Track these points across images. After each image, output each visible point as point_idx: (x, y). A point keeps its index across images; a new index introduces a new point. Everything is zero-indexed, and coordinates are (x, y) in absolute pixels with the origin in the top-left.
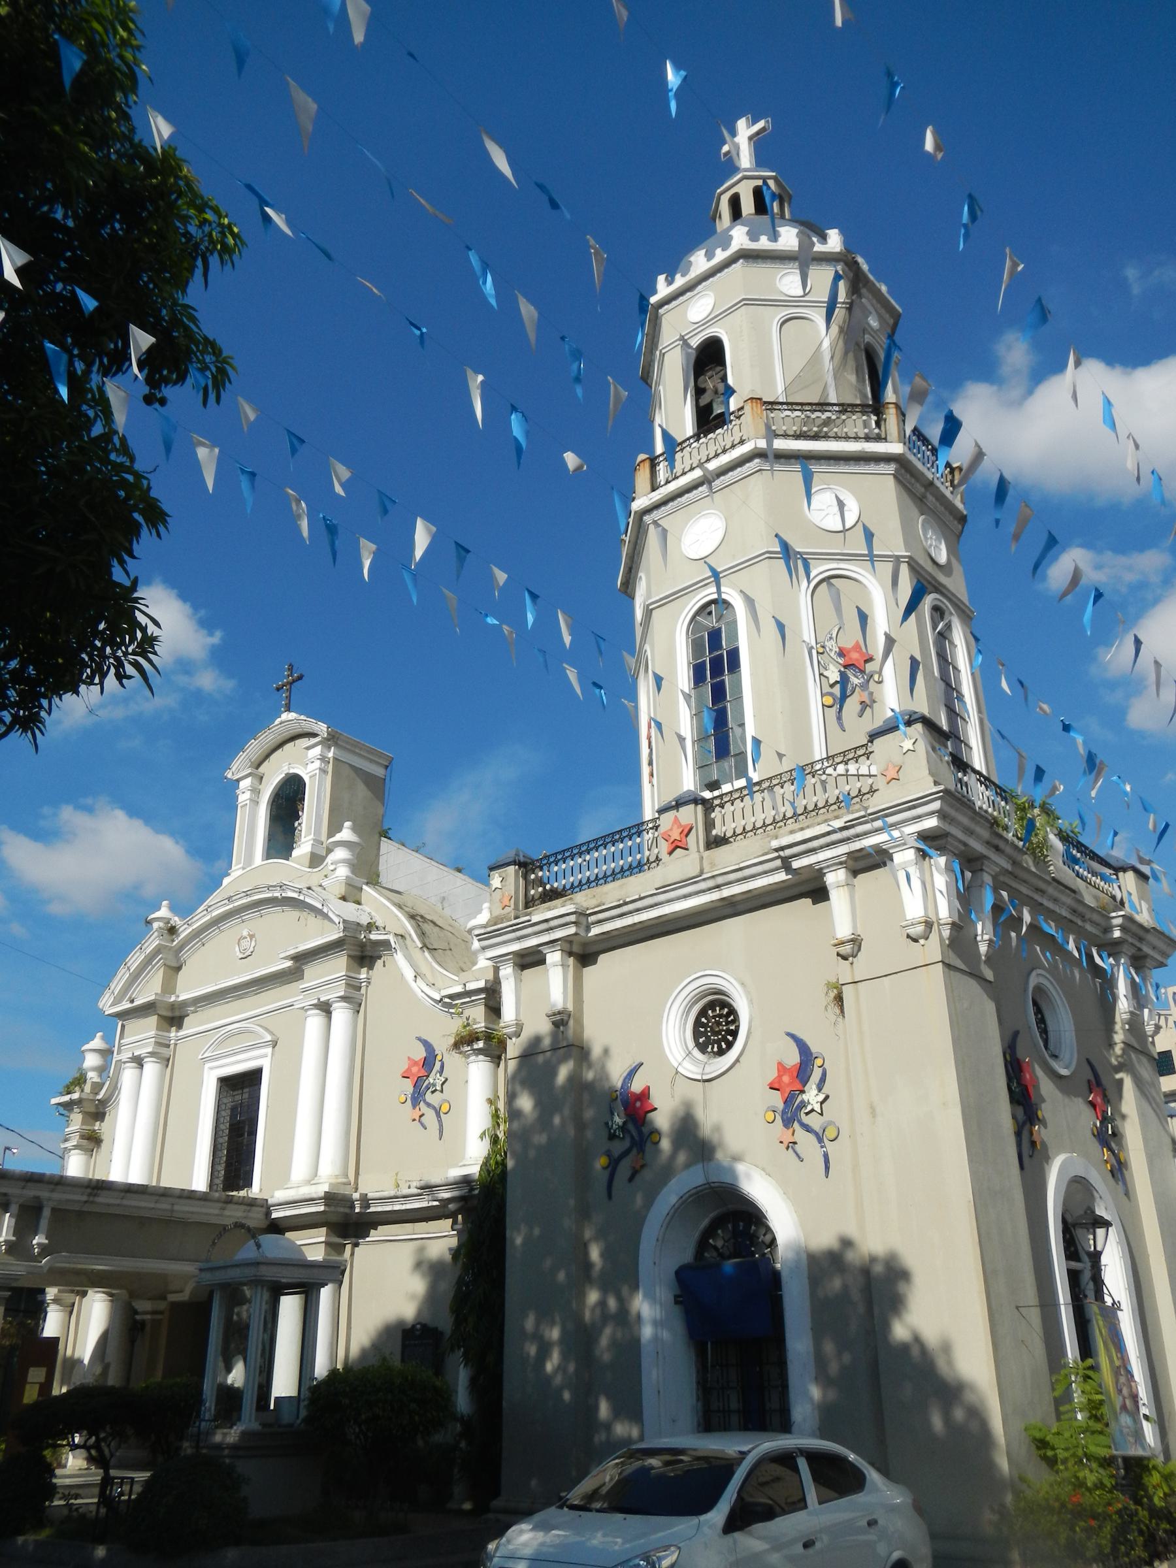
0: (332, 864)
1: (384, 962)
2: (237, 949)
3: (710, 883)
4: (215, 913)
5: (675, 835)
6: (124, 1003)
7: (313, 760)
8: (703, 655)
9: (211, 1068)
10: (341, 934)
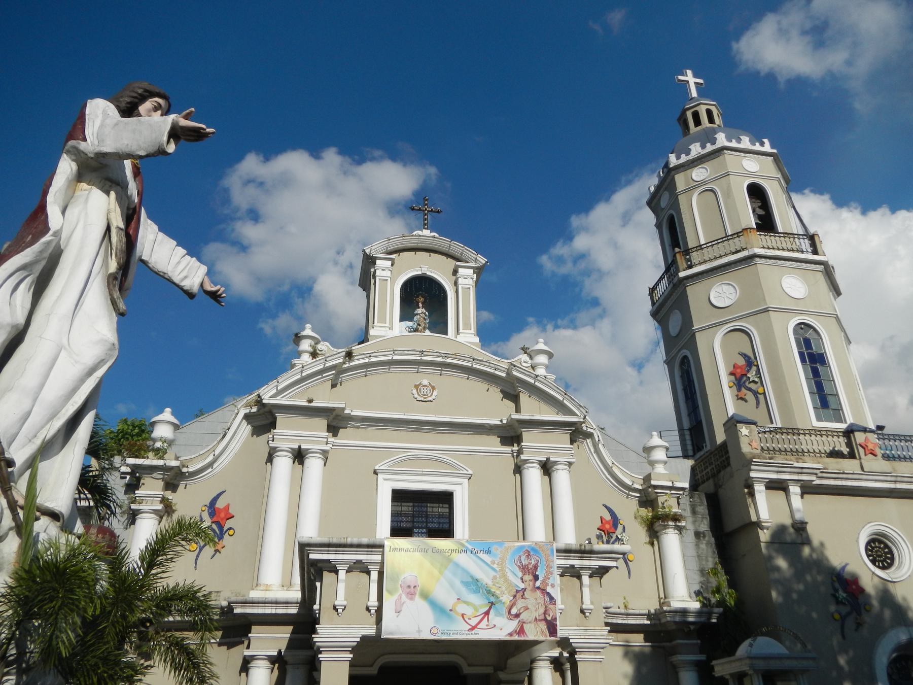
0: (525, 362)
1: (578, 446)
2: (415, 391)
3: (893, 479)
4: (396, 357)
5: (870, 446)
6: (278, 398)
7: (465, 277)
8: (802, 348)
9: (385, 479)
10: (582, 420)
